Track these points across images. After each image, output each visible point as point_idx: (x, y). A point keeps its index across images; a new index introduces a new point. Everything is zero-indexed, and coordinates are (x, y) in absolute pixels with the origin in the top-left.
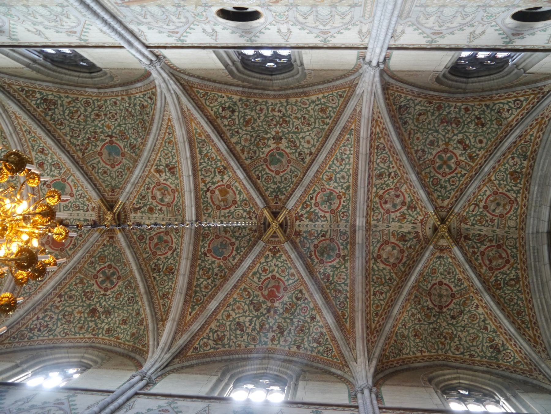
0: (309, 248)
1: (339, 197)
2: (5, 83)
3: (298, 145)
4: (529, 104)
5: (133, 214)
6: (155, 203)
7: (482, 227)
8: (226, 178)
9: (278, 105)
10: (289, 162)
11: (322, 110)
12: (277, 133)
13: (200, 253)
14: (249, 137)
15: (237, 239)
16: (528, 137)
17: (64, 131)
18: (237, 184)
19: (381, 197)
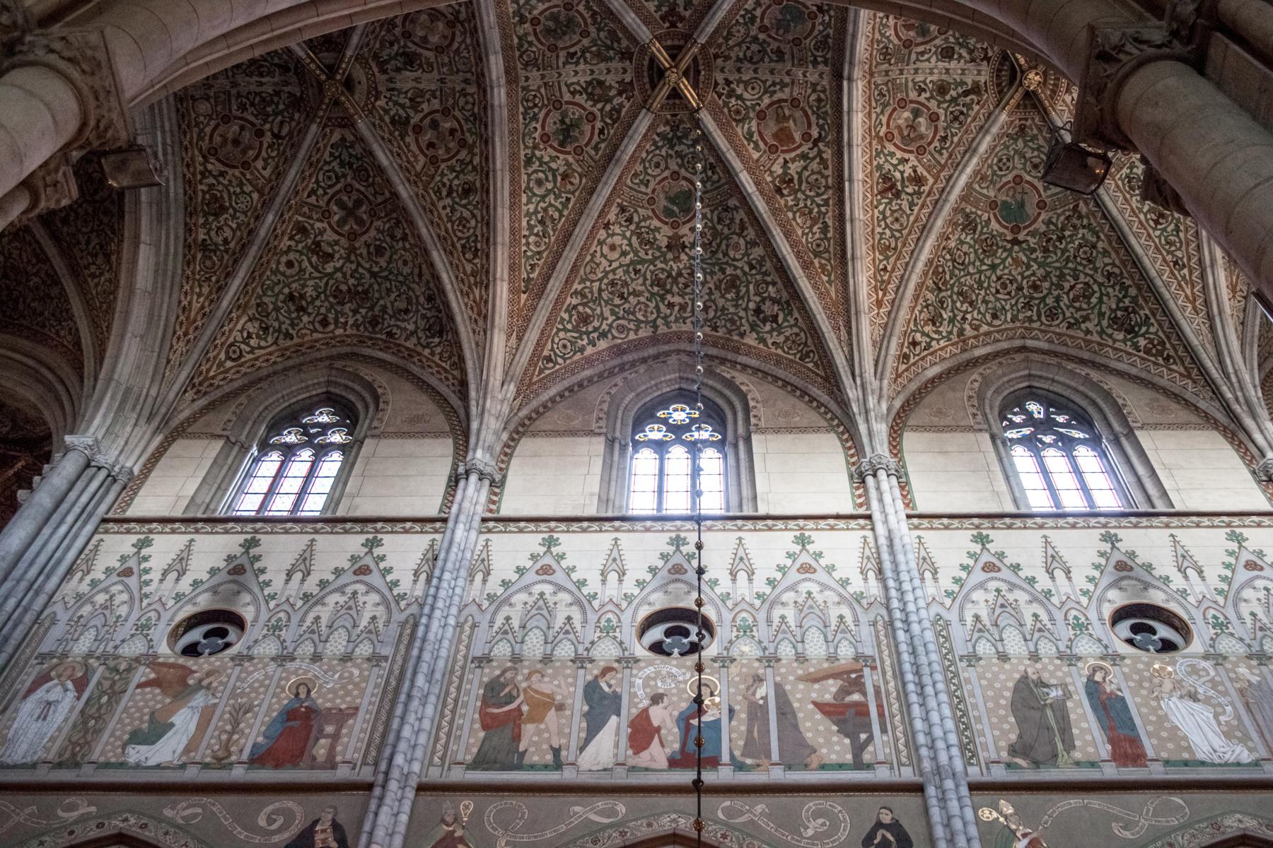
0: (599, 30)
1: (545, 138)
2: (1194, 382)
3: (634, 239)
4: (215, 358)
5: (982, 79)
6: (933, 104)
7: (258, 90)
8: (777, 169)
9: (672, 318)
10: (652, 201)
11: (585, 319)
12: (677, 259)
13: (832, 13)
14: (731, 253)
15: (755, 39)
16: (206, 290)
17: (1107, 260)
18: (756, 155)
19: (463, 143)
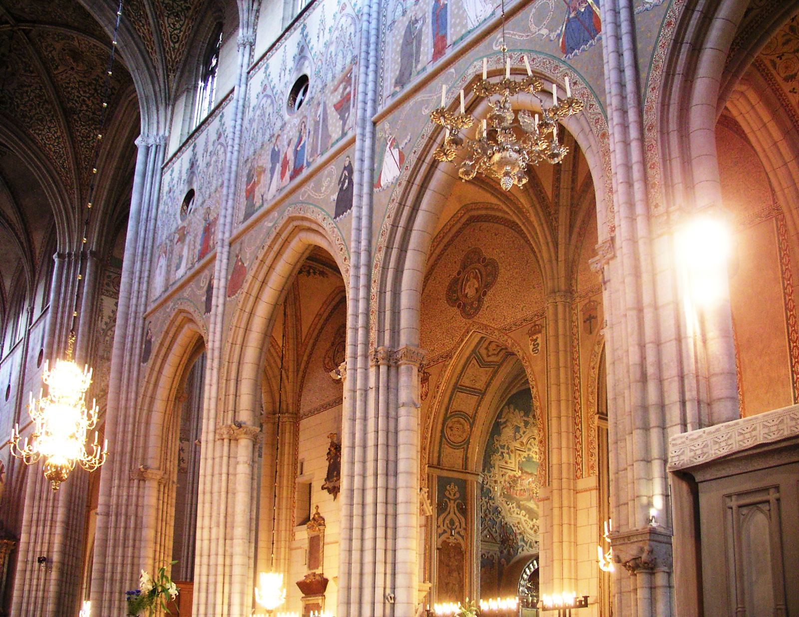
16: (144, 22)
